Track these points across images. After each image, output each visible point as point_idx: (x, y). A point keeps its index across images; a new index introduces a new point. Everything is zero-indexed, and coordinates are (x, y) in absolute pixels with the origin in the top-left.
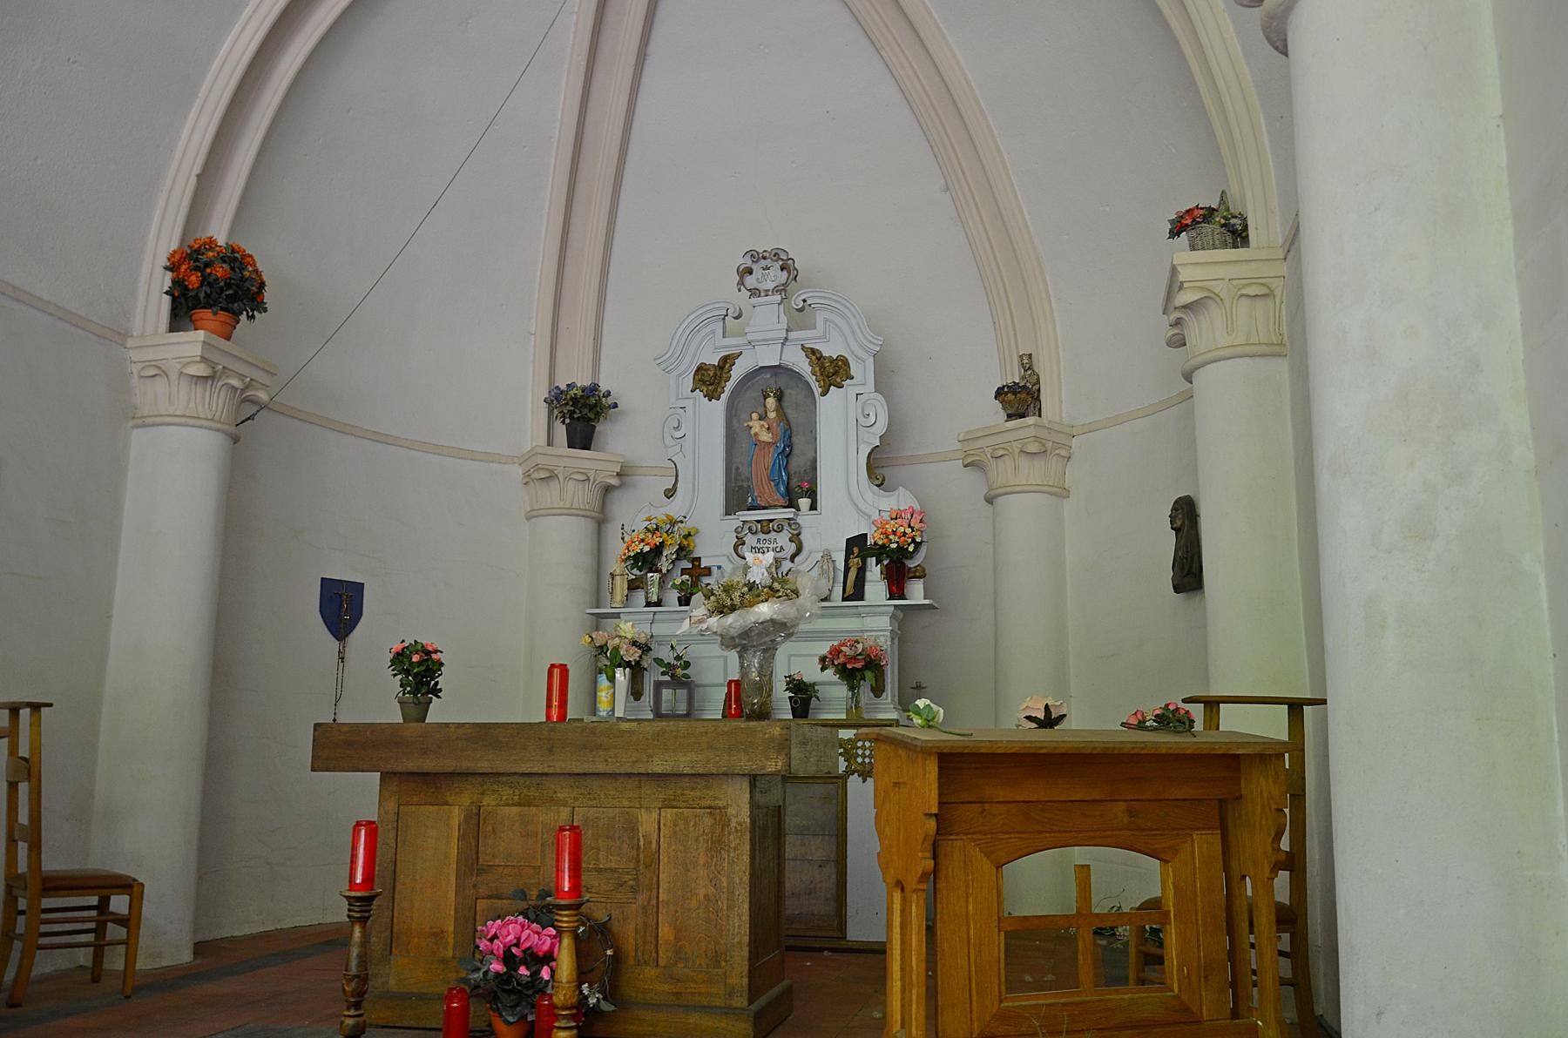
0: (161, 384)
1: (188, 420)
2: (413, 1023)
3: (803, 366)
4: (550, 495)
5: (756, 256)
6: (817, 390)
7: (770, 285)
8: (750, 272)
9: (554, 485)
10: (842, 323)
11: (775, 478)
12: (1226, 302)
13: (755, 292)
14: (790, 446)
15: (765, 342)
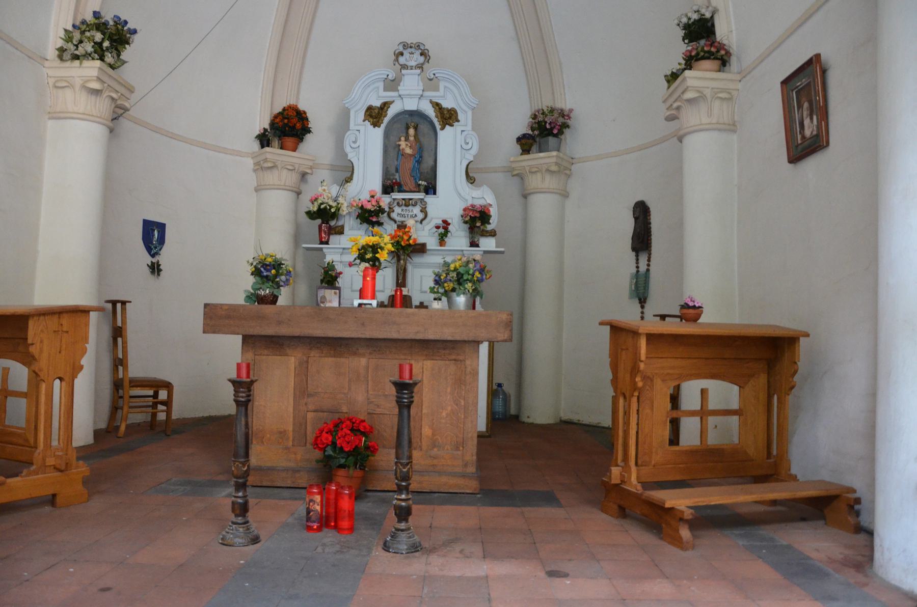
0: (68, 93)
1: (85, 117)
2: (269, 484)
3: (431, 112)
4: (271, 178)
5: (406, 46)
6: (438, 127)
7: (413, 63)
8: (402, 54)
9: (275, 172)
10: (456, 91)
11: (411, 172)
12: (709, 100)
13: (404, 67)
14: (421, 157)
15: (411, 96)
